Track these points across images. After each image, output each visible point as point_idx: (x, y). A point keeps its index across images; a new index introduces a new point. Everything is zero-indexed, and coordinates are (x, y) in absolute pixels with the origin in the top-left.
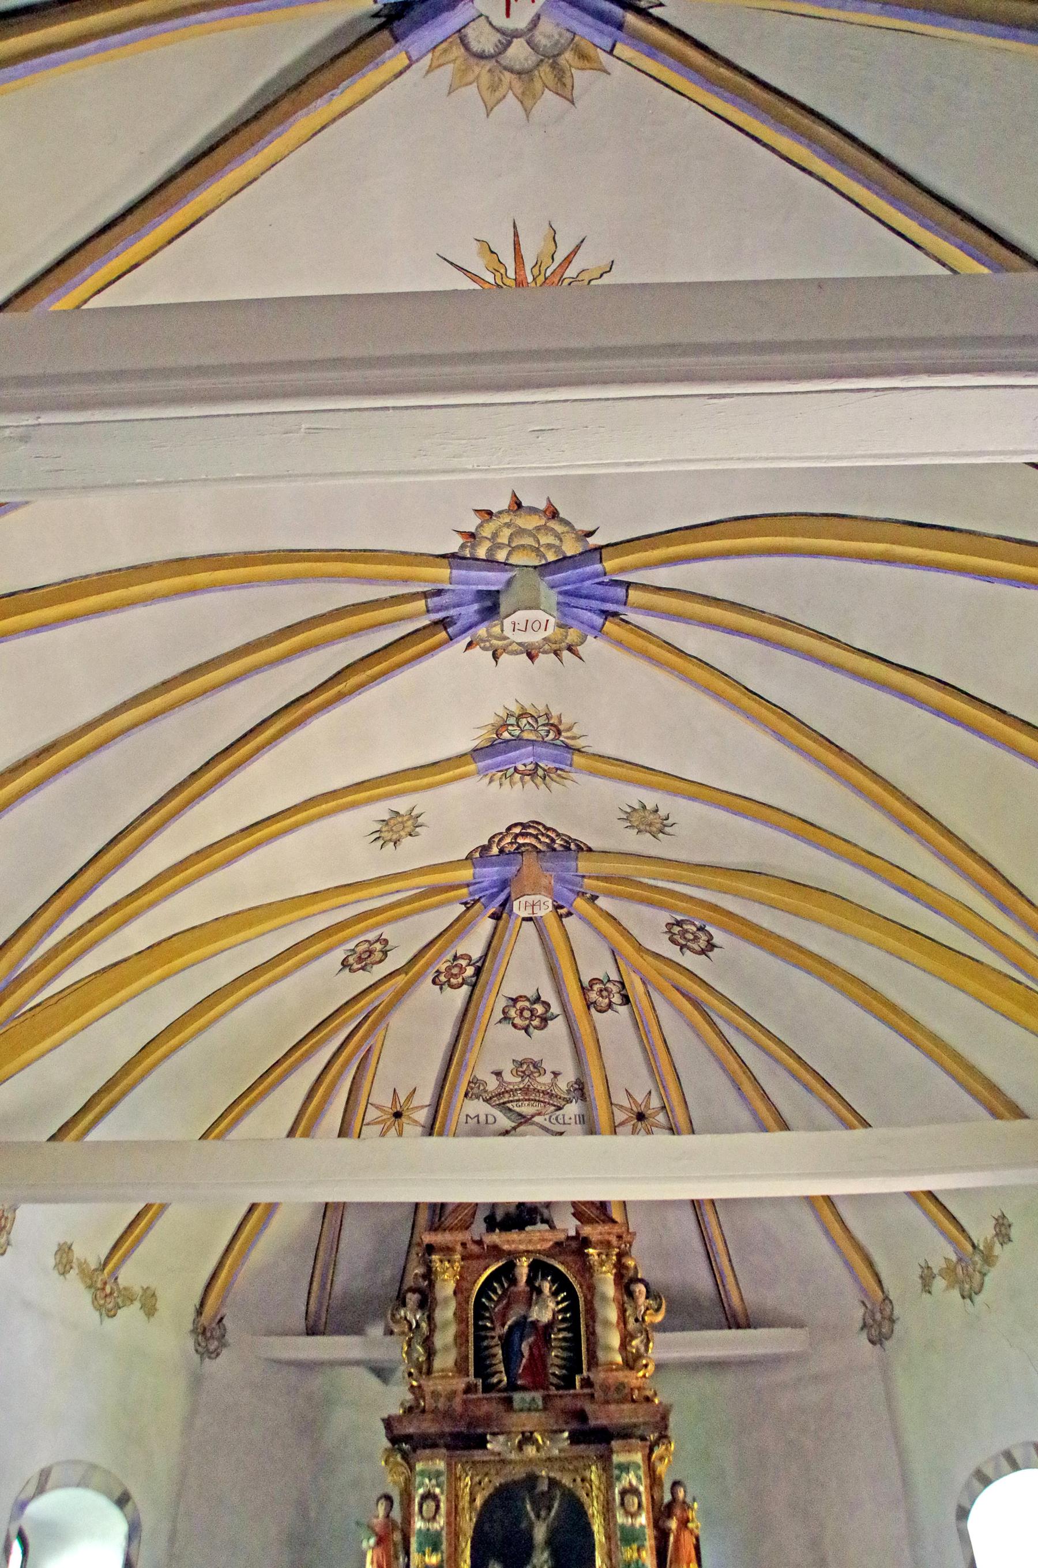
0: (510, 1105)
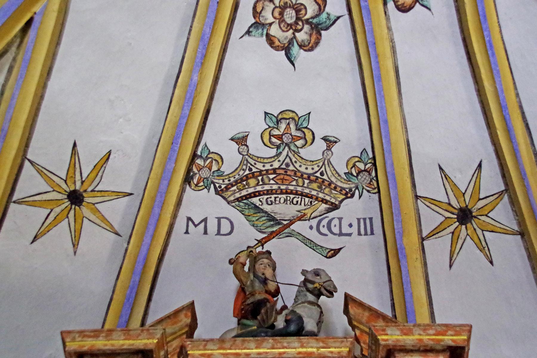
0: (255, 200)
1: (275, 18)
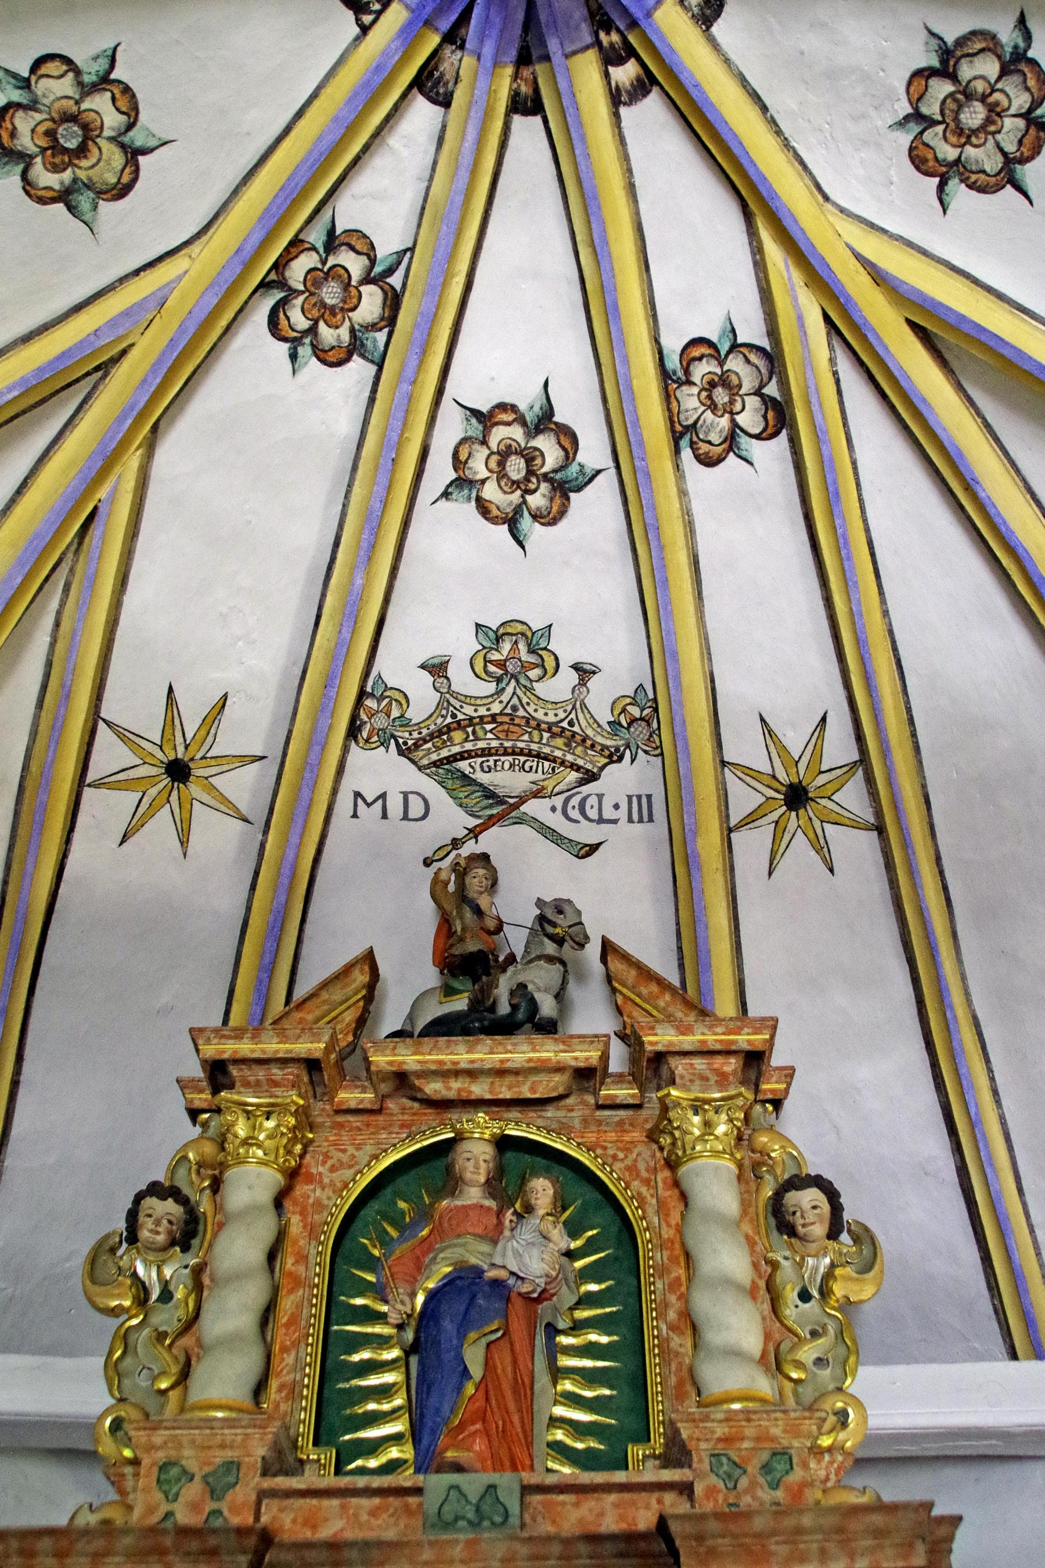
0: (464, 765)
1: (491, 471)
